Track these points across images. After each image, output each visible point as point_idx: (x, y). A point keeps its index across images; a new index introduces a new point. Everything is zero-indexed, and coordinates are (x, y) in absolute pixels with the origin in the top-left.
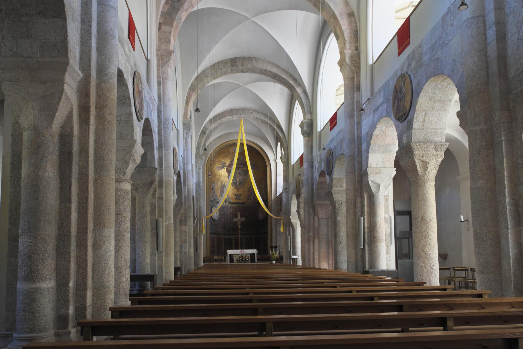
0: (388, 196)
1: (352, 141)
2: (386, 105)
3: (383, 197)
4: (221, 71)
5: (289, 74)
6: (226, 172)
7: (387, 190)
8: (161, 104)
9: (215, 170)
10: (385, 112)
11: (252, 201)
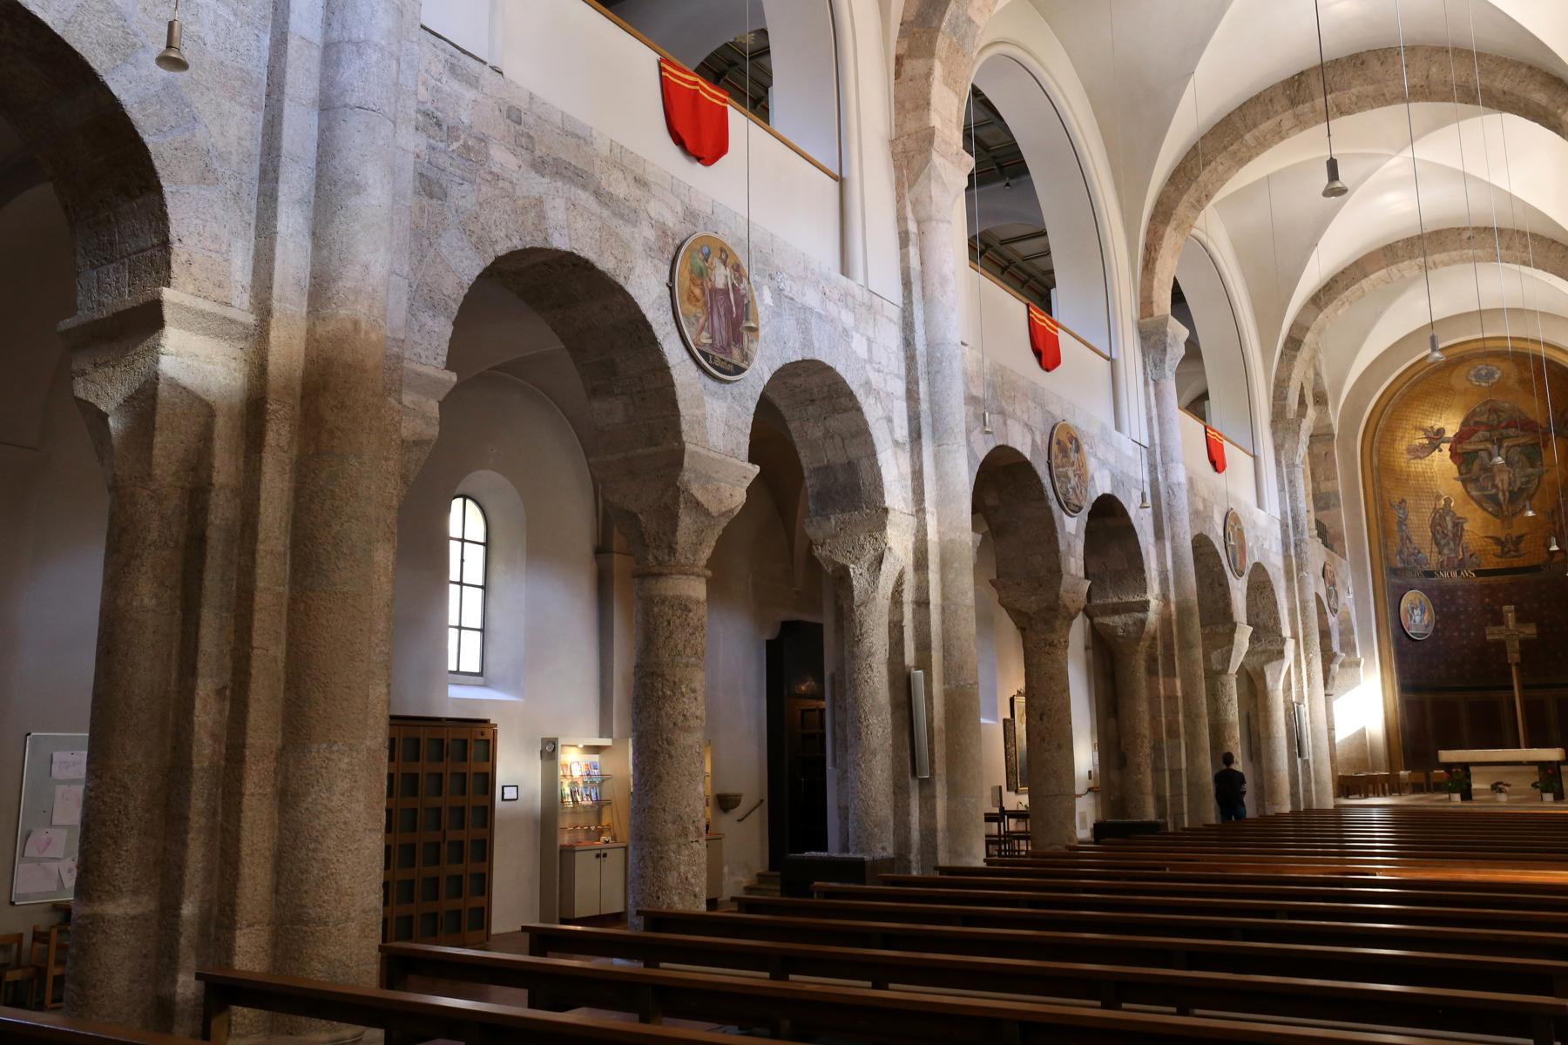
4: (1256, 132)
5: (1524, 70)
8: (911, 302)
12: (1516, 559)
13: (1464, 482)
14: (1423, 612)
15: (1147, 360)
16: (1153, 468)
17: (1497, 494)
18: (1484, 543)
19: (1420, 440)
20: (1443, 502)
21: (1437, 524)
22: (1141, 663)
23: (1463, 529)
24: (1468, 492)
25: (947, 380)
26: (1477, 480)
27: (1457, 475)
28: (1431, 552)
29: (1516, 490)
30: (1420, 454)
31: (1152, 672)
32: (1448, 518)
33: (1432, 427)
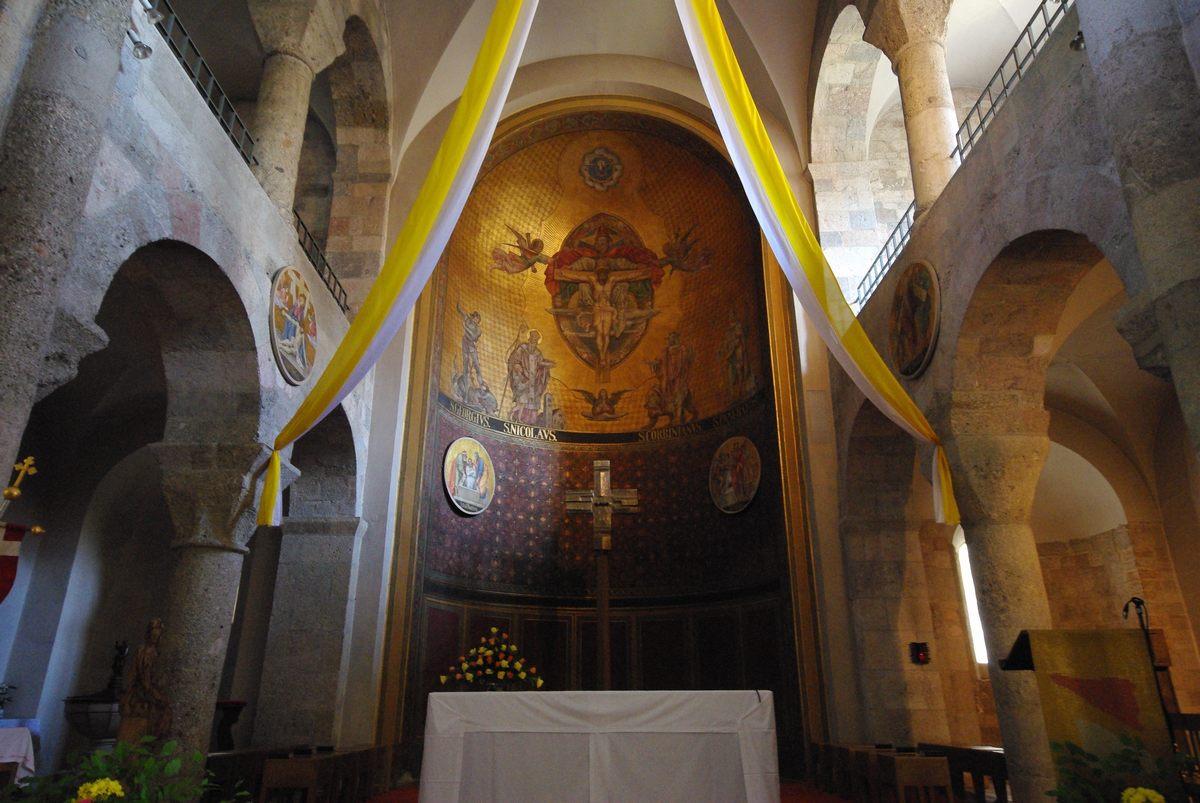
6: (544, 289)
11: (677, 420)
12: (610, 422)
13: (558, 317)
14: (480, 473)
17: (595, 338)
18: (572, 398)
19: (510, 246)
20: (528, 336)
23: (548, 374)
26: (573, 318)
27: (550, 307)
28: (504, 395)
29: (618, 336)
30: (508, 266)
32: (531, 357)
33: (528, 235)
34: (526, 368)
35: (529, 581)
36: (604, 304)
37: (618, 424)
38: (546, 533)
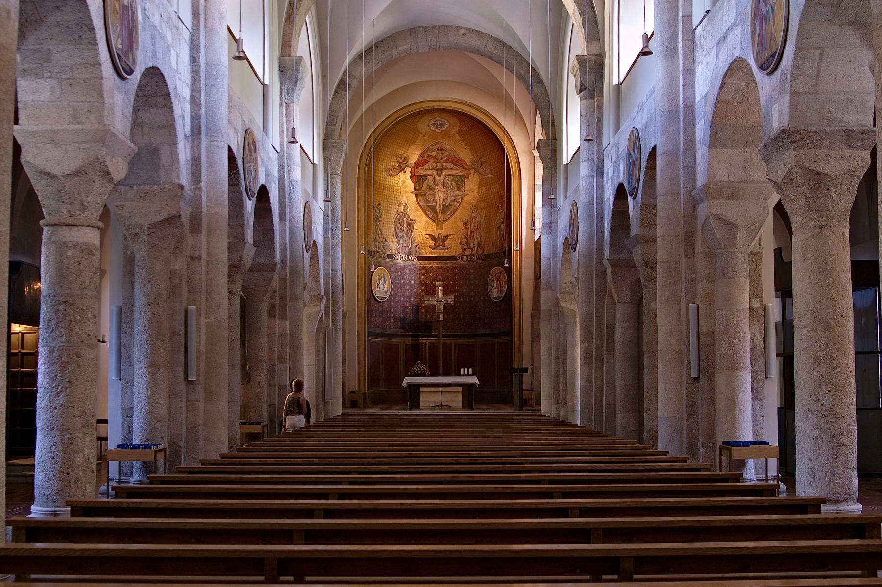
0: (759, 253)
1: (672, 114)
2: (740, 28)
3: (747, 256)
7: (757, 238)
8: (199, 29)
9: (382, 175)
10: (739, 46)
11: (475, 252)
12: (443, 251)
13: (417, 196)
14: (385, 282)
15: (283, 87)
16: (281, 168)
17: (436, 206)
18: (425, 239)
21: (398, 222)
22: (264, 308)
23: (413, 227)
24: (418, 203)
25: (220, 93)
26: (425, 195)
27: (413, 190)
29: (447, 205)
31: (271, 315)
32: (405, 219)
34: (402, 225)
35: (407, 328)
36: (439, 187)
37: (447, 252)
38: (413, 305)
